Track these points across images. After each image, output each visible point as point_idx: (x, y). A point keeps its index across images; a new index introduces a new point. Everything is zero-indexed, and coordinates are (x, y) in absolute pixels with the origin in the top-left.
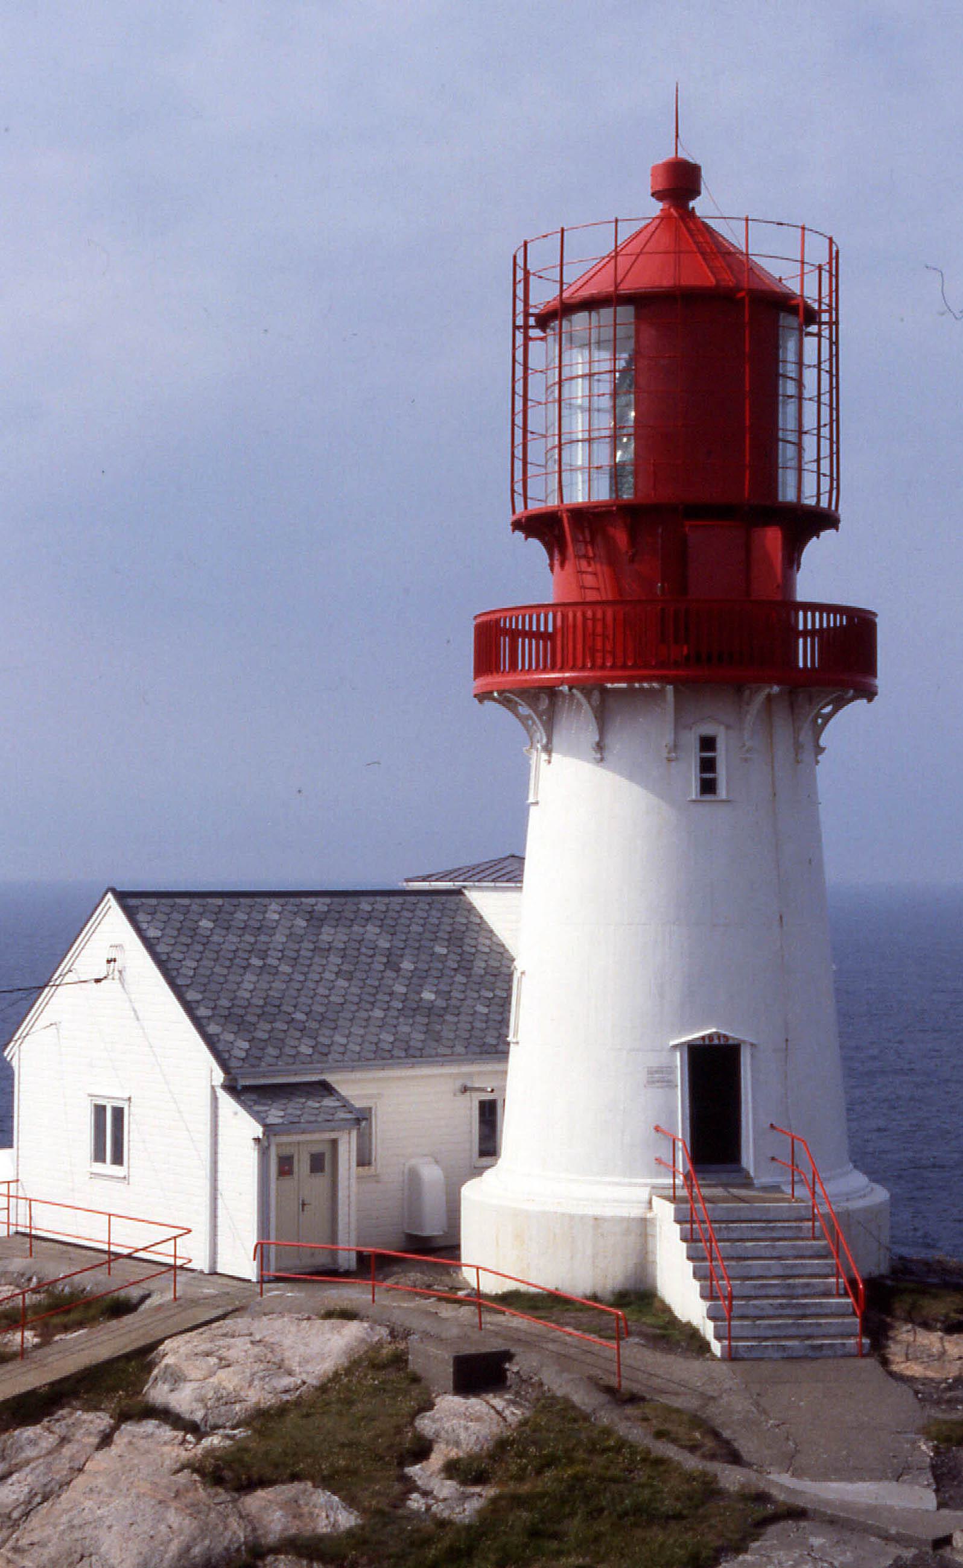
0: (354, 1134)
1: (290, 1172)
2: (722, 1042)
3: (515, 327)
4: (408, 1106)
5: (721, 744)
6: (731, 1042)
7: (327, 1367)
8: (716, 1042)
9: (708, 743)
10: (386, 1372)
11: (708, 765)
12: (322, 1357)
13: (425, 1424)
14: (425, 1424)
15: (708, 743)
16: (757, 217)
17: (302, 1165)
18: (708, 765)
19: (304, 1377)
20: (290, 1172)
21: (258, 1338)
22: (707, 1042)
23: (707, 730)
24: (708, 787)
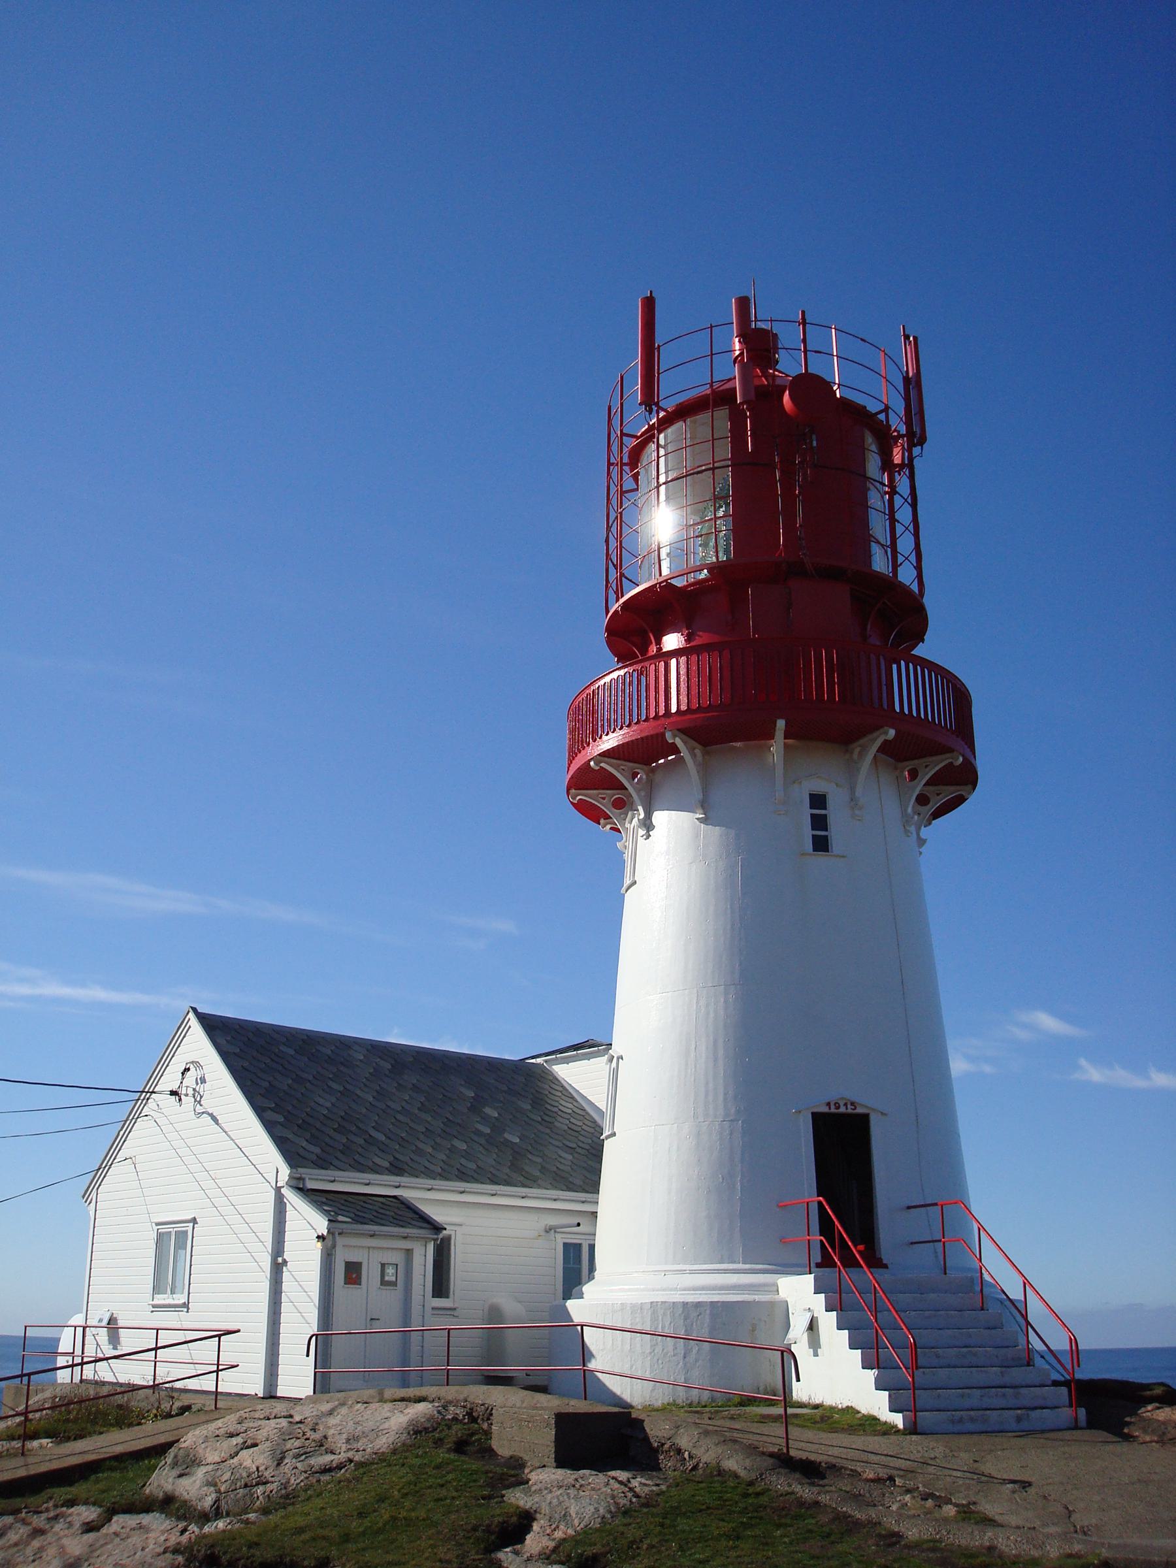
0: (431, 1247)
2: (849, 1111)
3: (609, 464)
4: (491, 1228)
6: (859, 1110)
7: (383, 1443)
8: (842, 1110)
9: (818, 801)
10: (461, 1441)
11: (819, 822)
12: (377, 1432)
13: (517, 1498)
14: (517, 1498)
15: (818, 801)
17: (371, 1274)
18: (819, 822)
19: (350, 1454)
21: (297, 1418)
22: (833, 1110)
23: (819, 786)
24: (821, 845)
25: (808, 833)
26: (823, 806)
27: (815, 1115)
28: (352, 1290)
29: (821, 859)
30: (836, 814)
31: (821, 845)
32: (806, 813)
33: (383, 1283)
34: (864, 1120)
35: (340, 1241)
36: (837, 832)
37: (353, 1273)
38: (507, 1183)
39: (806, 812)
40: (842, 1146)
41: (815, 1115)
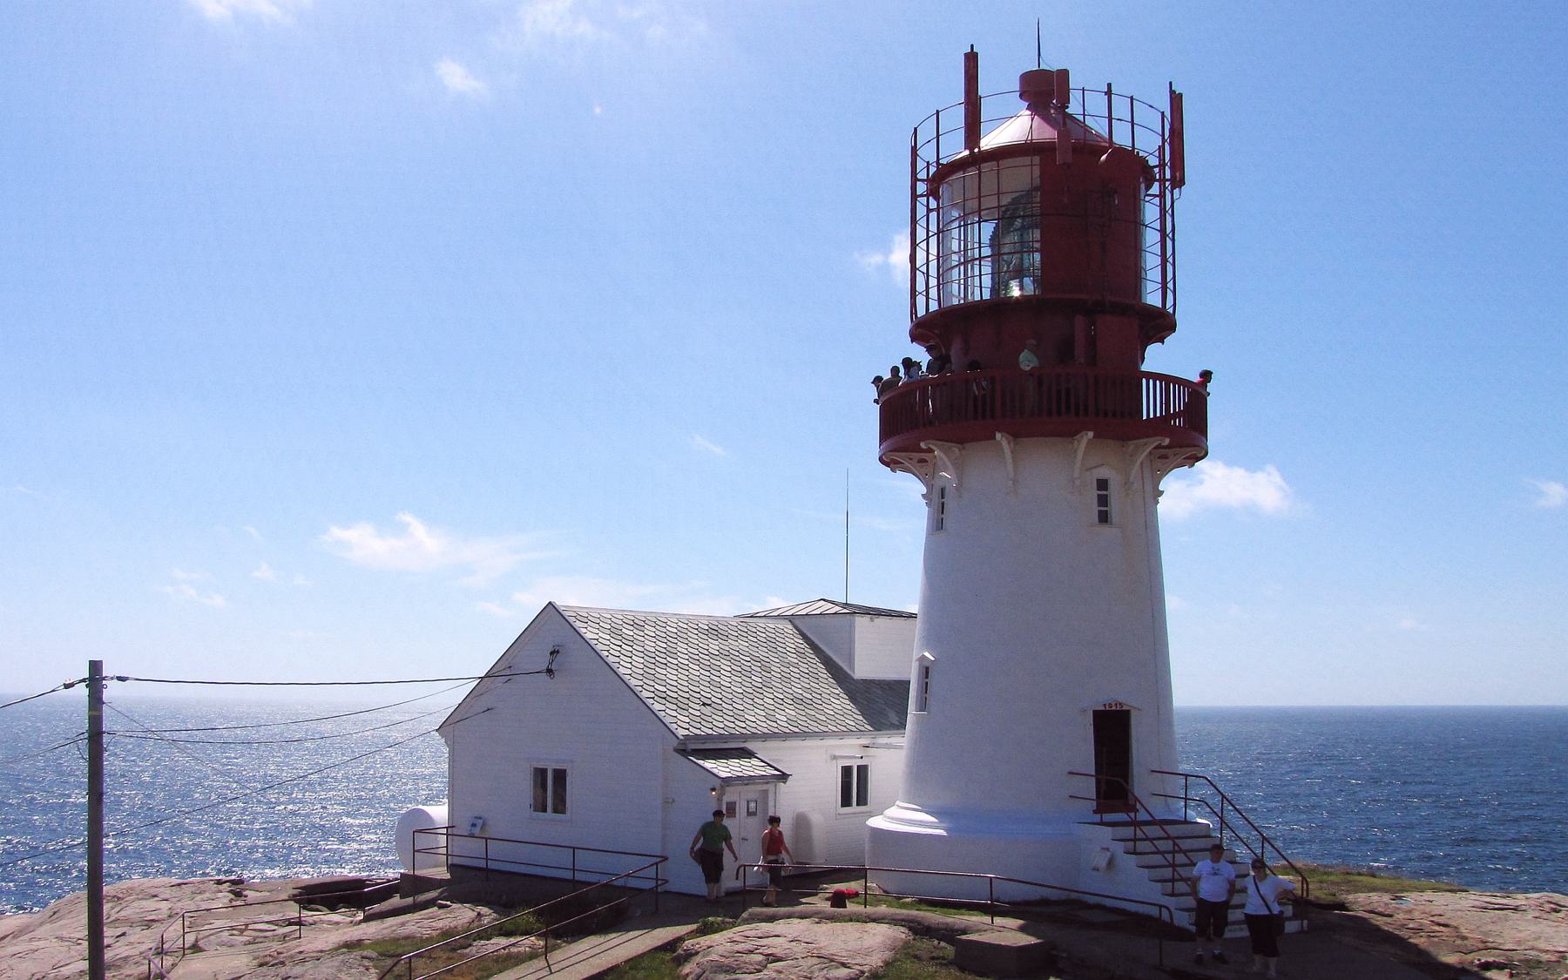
5: (1113, 485)
9: (1102, 484)
11: (1103, 501)
15: (1102, 484)
18: (1103, 501)
23: (1104, 473)
24: (1104, 518)
25: (1095, 508)
26: (1106, 489)
29: (1105, 530)
30: (1114, 492)
31: (1104, 518)
34: (1127, 713)
36: (1114, 507)
39: (1095, 493)
40: (1112, 730)
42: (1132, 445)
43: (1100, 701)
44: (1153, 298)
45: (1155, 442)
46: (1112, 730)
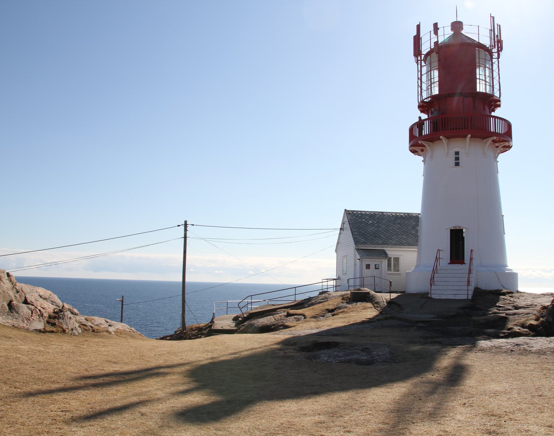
0: (387, 260)
1: (369, 268)
9: (457, 153)
11: (457, 159)
15: (457, 153)
16: (477, 32)
17: (372, 267)
18: (457, 159)
20: (369, 268)
23: (457, 150)
24: (457, 164)
25: (453, 161)
26: (458, 154)
27: (451, 230)
28: (368, 270)
29: (457, 168)
31: (457, 164)
32: (453, 157)
33: (376, 268)
35: (363, 260)
36: (460, 161)
37: (368, 267)
38: (413, 245)
40: (457, 237)
41: (451, 230)
42: (485, 140)
43: (452, 226)
44: (481, 88)
45: (492, 139)
46: (457, 237)
